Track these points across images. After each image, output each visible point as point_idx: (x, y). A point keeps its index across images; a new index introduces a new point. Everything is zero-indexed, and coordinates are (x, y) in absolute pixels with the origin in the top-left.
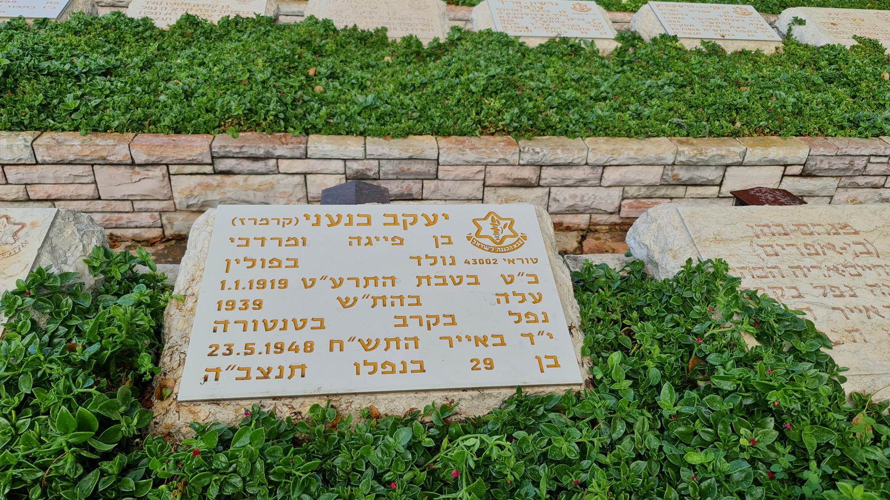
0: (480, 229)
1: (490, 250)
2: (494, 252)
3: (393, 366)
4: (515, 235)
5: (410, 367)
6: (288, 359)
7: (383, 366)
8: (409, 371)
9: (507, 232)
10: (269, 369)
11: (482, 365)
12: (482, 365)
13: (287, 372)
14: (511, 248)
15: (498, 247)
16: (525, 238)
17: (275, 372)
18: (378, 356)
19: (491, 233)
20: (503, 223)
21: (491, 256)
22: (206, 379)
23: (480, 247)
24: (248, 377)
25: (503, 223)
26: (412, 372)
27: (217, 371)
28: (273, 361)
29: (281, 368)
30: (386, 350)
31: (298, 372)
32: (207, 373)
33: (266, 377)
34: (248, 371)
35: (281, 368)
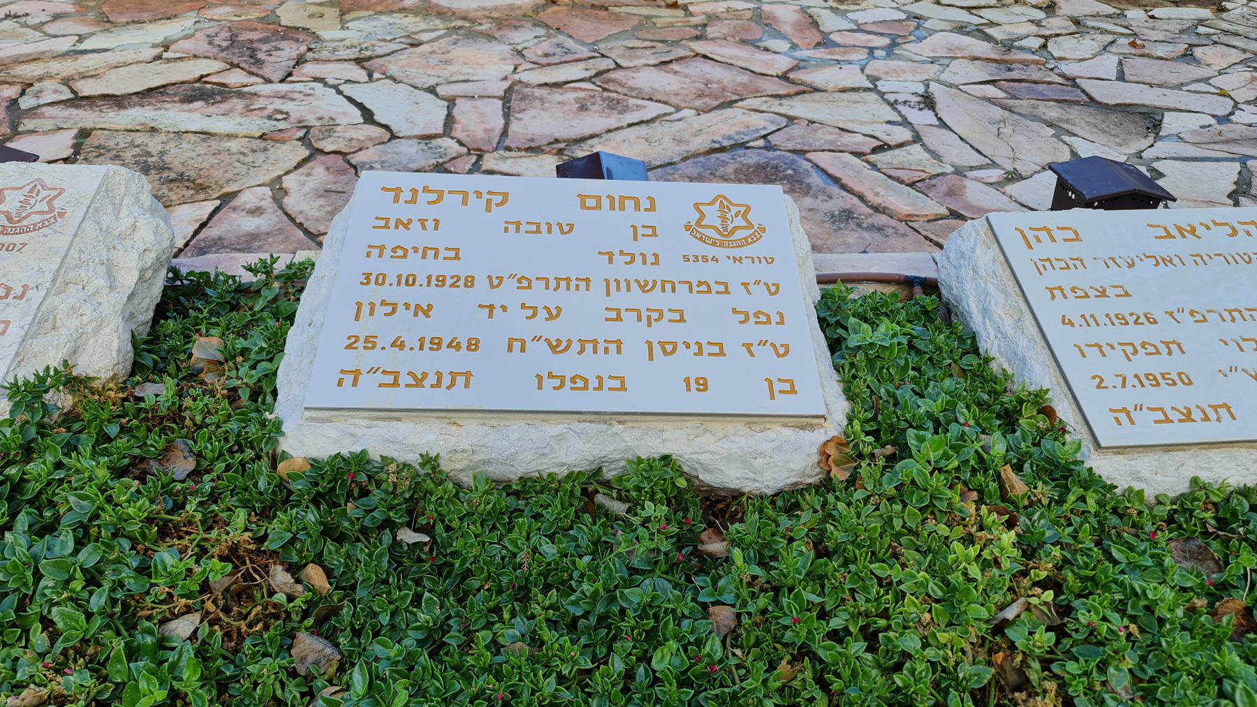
0: (703, 215)
1: (714, 244)
2: (722, 245)
3: (586, 381)
4: (750, 226)
5: (607, 383)
6: (447, 361)
7: (573, 380)
8: (605, 387)
9: (739, 221)
10: (425, 375)
13: (446, 380)
14: (746, 242)
15: (724, 238)
17: (432, 379)
18: (567, 364)
19: (717, 223)
22: (340, 383)
23: (700, 239)
24: (395, 384)
25: (734, 210)
26: (610, 389)
27: (357, 373)
28: (428, 362)
29: (439, 375)
30: (579, 353)
31: (460, 380)
32: (342, 376)
33: (418, 382)
34: (396, 375)
35: (439, 375)
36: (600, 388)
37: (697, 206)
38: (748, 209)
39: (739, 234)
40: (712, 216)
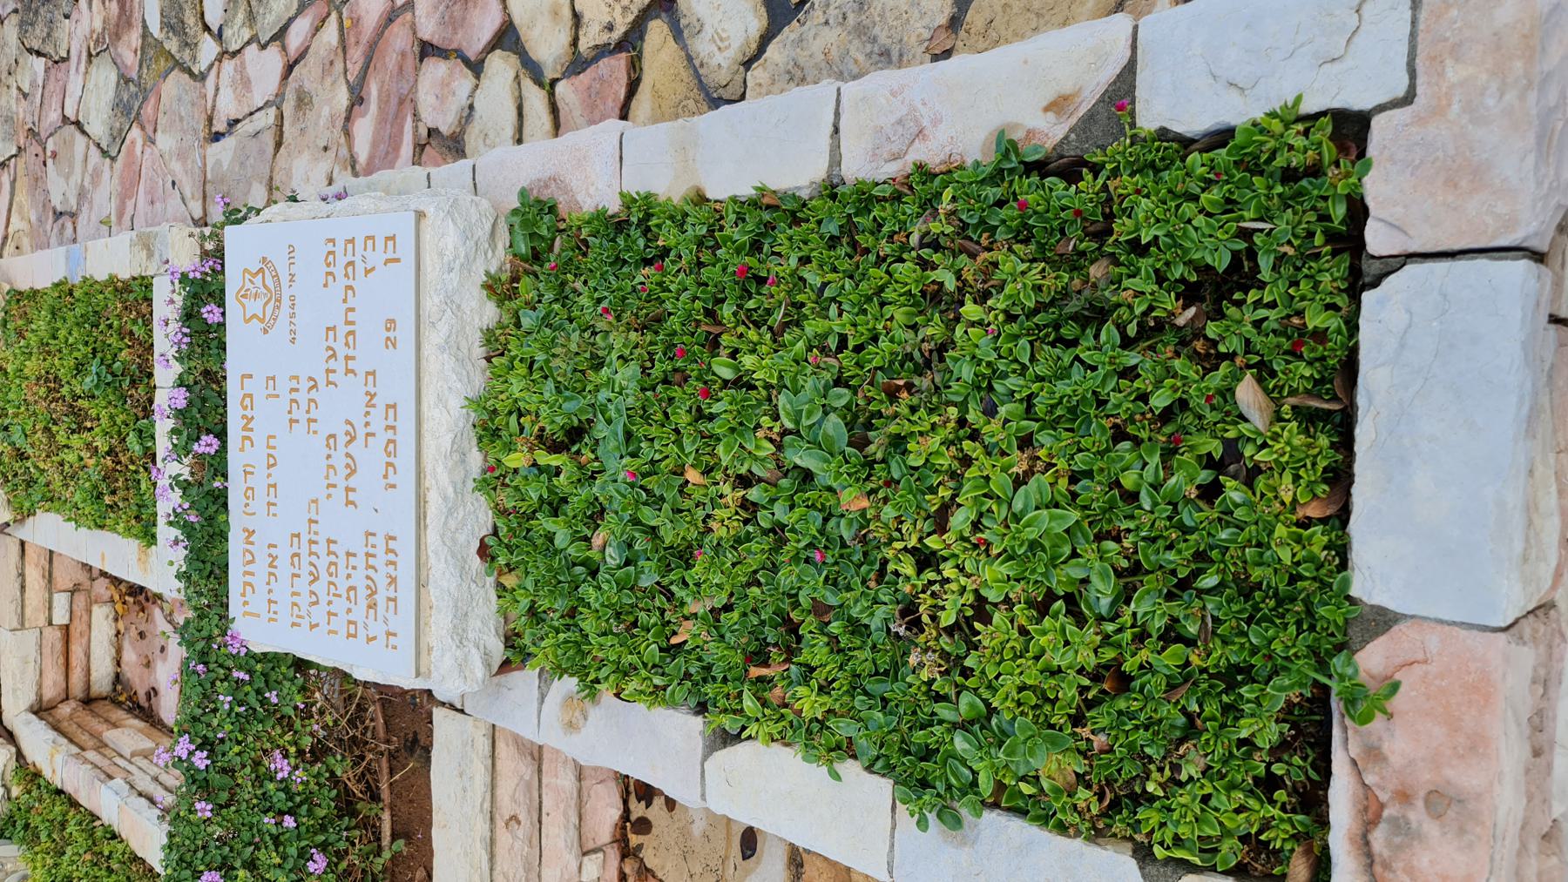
0: (254, 316)
5: (391, 422)
11: (391, 334)
12: (391, 334)
13: (391, 557)
16: (264, 259)
20: (248, 285)
21: (286, 302)
24: (394, 600)
25: (248, 285)
27: (389, 634)
33: (393, 580)
36: (393, 428)
37: (247, 321)
38: (245, 271)
39: (269, 282)
40: (255, 307)
